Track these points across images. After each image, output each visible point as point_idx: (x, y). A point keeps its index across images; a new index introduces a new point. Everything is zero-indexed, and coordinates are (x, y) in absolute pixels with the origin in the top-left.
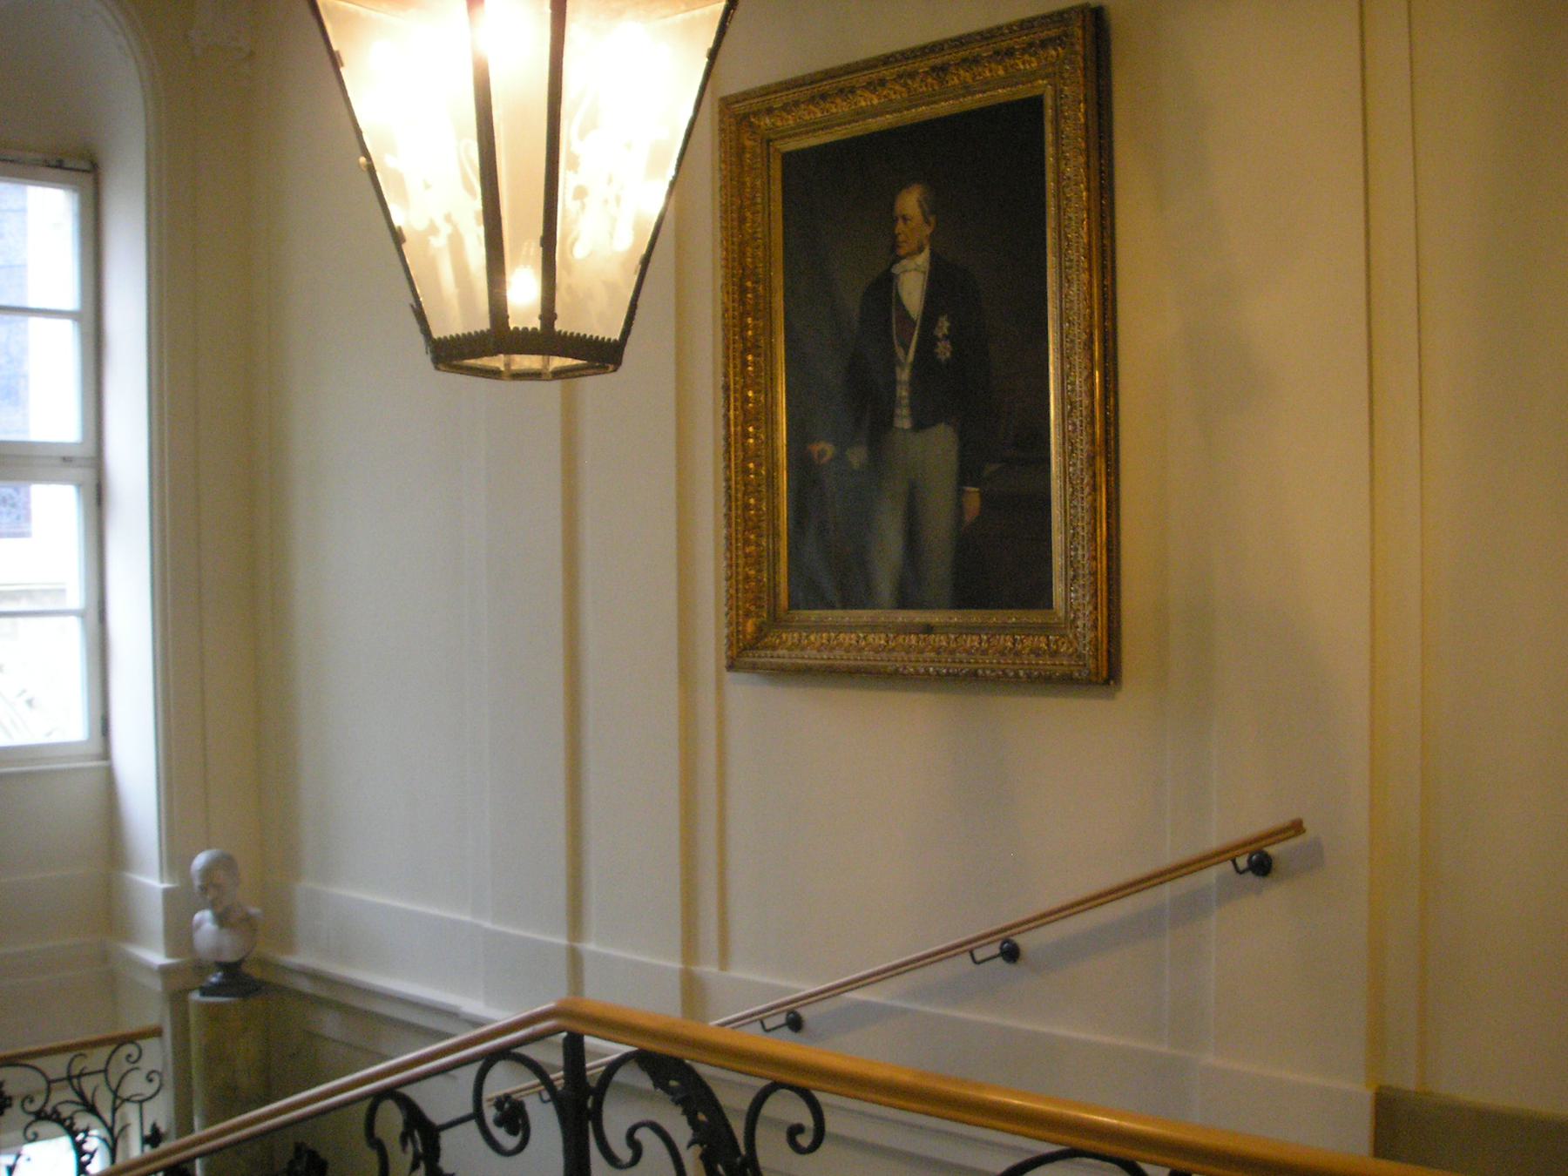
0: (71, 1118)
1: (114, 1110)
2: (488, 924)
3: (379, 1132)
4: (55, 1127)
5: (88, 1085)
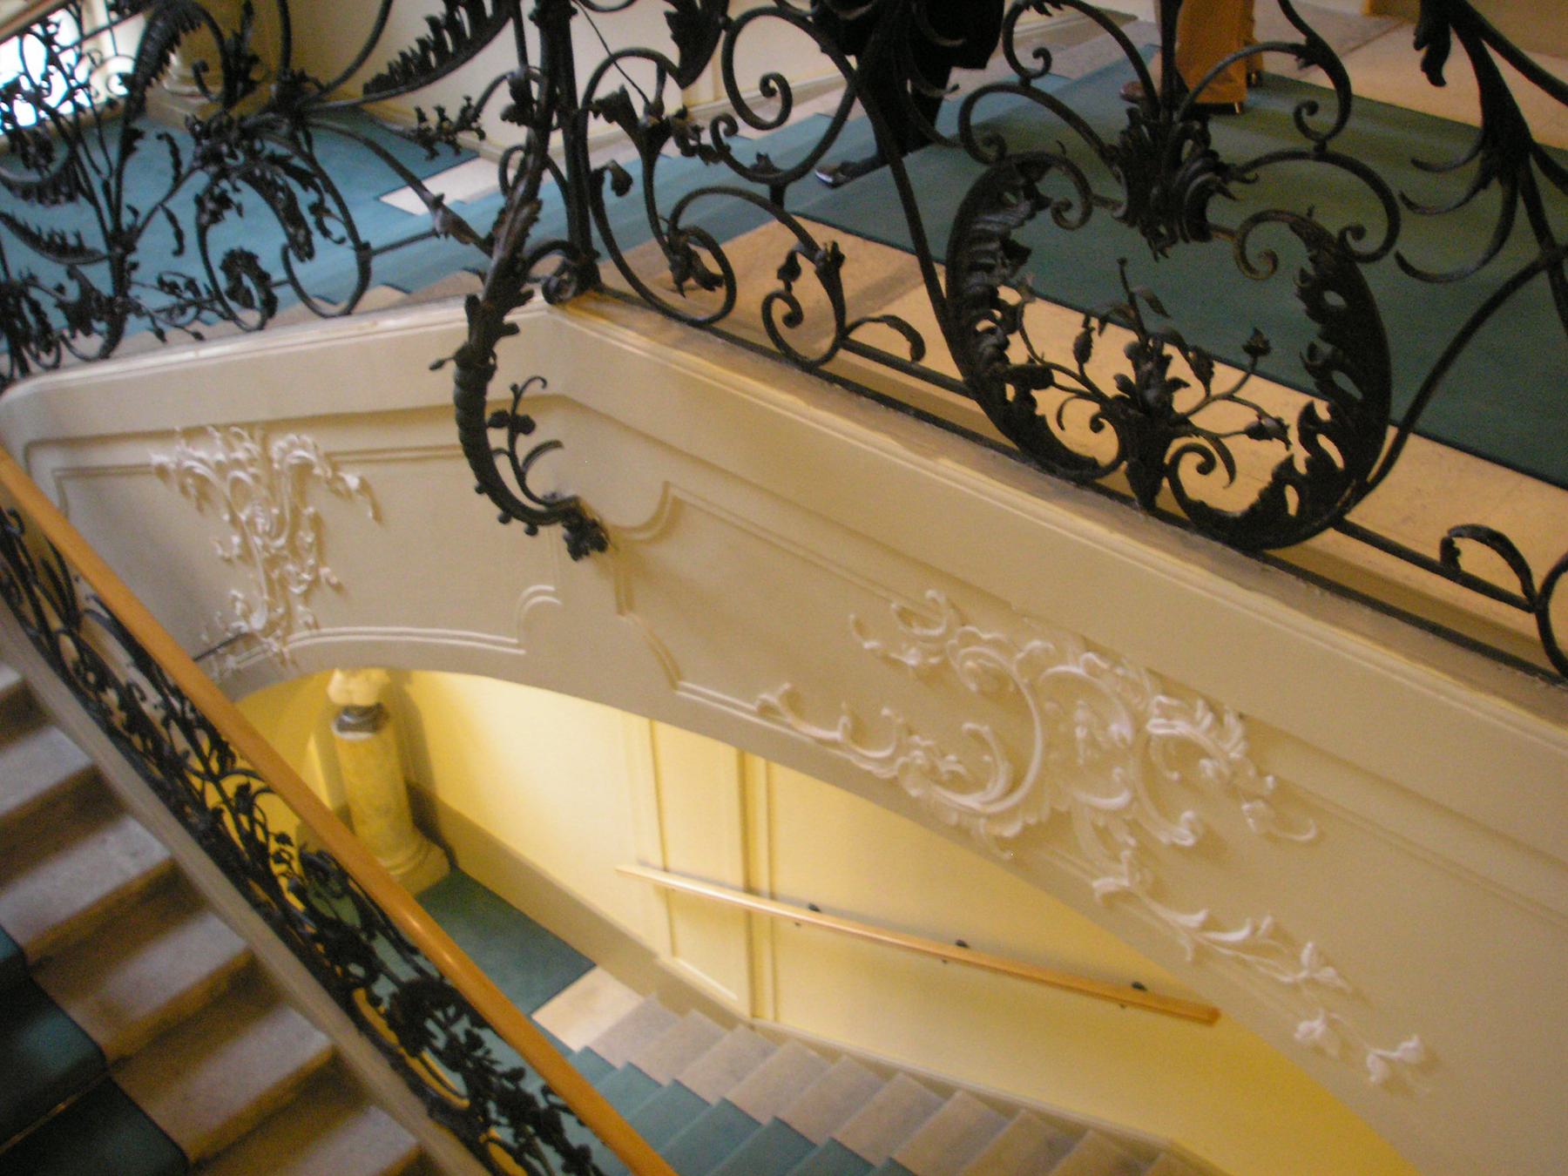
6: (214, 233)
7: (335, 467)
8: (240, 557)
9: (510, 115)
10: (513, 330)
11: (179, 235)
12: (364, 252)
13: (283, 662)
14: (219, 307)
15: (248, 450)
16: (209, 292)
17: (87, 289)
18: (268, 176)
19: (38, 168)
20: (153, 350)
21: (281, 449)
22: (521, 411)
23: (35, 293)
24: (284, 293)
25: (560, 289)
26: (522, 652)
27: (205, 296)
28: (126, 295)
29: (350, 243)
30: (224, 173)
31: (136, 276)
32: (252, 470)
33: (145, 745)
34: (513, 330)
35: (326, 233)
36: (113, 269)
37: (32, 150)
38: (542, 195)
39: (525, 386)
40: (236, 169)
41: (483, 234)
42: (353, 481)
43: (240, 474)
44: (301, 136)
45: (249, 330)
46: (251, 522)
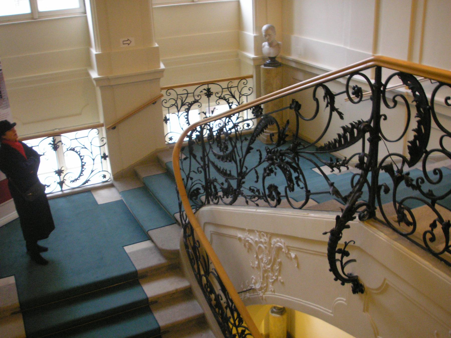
1: (240, 97)
2: (348, 48)
3: (317, 96)
4: (224, 102)
5: (233, 90)
6: (267, 178)
7: (289, 250)
8: (256, 267)
9: (358, 166)
10: (348, 227)
11: (258, 177)
12: (308, 193)
13: (262, 299)
14: (264, 197)
15: (265, 240)
16: (263, 194)
17: (230, 186)
18: (285, 167)
19: (224, 152)
20: (244, 206)
21: (274, 241)
22: (346, 249)
23: (215, 184)
24: (284, 200)
25: (364, 217)
26: (332, 315)
27: (261, 195)
28: (240, 190)
29: (304, 189)
30: (273, 164)
31: (243, 185)
32: (265, 245)
33: (219, 311)
34: (348, 227)
35: (298, 185)
36: (238, 182)
37: (223, 147)
38: (363, 190)
39: (349, 243)
40: (277, 163)
41: (343, 196)
42: (293, 255)
43: (261, 245)
44: (296, 159)
45: (272, 207)
46: (262, 259)
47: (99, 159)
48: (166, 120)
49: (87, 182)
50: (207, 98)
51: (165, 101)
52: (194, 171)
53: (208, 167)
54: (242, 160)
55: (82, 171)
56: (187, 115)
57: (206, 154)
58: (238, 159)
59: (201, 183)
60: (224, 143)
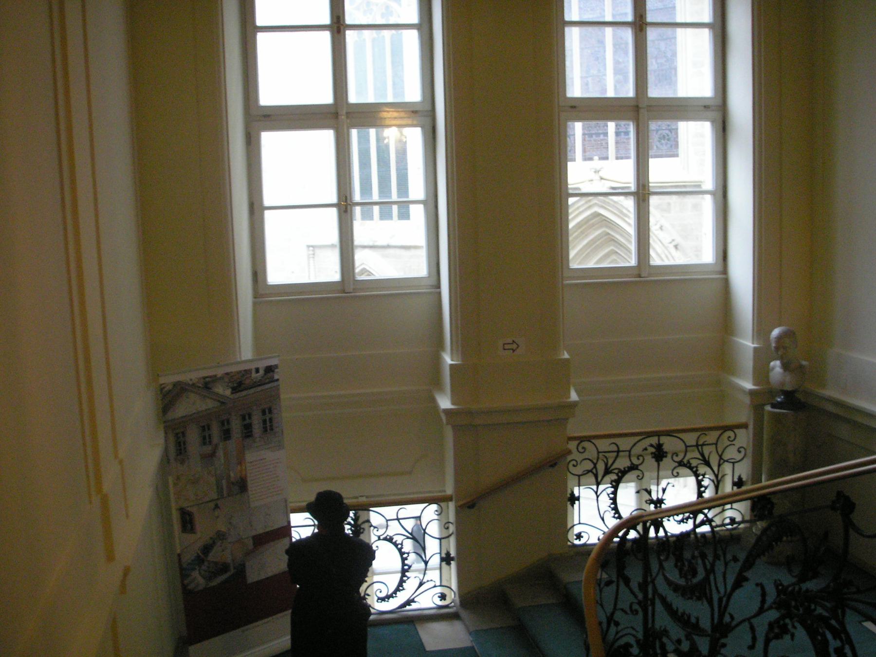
0: (697, 467)
1: (719, 465)
4: (688, 471)
5: (706, 450)
6: (773, 644)
11: (754, 639)
17: (694, 648)
18: (815, 626)
19: (687, 579)
23: (665, 640)
31: (723, 651)
37: (686, 569)
44: (840, 611)
47: (435, 561)
48: (573, 499)
49: (409, 602)
50: (656, 464)
51: (574, 463)
52: (622, 610)
53: (653, 604)
54: (725, 599)
55: (401, 582)
56: (615, 493)
57: (649, 579)
58: (715, 597)
59: (634, 632)
60: (690, 562)
